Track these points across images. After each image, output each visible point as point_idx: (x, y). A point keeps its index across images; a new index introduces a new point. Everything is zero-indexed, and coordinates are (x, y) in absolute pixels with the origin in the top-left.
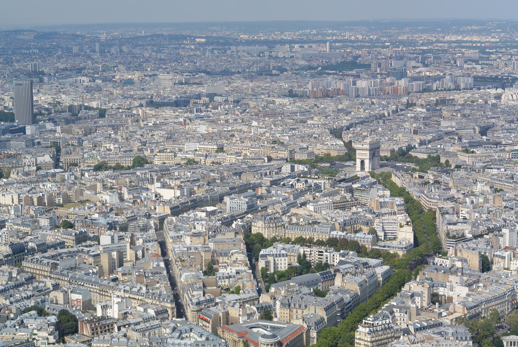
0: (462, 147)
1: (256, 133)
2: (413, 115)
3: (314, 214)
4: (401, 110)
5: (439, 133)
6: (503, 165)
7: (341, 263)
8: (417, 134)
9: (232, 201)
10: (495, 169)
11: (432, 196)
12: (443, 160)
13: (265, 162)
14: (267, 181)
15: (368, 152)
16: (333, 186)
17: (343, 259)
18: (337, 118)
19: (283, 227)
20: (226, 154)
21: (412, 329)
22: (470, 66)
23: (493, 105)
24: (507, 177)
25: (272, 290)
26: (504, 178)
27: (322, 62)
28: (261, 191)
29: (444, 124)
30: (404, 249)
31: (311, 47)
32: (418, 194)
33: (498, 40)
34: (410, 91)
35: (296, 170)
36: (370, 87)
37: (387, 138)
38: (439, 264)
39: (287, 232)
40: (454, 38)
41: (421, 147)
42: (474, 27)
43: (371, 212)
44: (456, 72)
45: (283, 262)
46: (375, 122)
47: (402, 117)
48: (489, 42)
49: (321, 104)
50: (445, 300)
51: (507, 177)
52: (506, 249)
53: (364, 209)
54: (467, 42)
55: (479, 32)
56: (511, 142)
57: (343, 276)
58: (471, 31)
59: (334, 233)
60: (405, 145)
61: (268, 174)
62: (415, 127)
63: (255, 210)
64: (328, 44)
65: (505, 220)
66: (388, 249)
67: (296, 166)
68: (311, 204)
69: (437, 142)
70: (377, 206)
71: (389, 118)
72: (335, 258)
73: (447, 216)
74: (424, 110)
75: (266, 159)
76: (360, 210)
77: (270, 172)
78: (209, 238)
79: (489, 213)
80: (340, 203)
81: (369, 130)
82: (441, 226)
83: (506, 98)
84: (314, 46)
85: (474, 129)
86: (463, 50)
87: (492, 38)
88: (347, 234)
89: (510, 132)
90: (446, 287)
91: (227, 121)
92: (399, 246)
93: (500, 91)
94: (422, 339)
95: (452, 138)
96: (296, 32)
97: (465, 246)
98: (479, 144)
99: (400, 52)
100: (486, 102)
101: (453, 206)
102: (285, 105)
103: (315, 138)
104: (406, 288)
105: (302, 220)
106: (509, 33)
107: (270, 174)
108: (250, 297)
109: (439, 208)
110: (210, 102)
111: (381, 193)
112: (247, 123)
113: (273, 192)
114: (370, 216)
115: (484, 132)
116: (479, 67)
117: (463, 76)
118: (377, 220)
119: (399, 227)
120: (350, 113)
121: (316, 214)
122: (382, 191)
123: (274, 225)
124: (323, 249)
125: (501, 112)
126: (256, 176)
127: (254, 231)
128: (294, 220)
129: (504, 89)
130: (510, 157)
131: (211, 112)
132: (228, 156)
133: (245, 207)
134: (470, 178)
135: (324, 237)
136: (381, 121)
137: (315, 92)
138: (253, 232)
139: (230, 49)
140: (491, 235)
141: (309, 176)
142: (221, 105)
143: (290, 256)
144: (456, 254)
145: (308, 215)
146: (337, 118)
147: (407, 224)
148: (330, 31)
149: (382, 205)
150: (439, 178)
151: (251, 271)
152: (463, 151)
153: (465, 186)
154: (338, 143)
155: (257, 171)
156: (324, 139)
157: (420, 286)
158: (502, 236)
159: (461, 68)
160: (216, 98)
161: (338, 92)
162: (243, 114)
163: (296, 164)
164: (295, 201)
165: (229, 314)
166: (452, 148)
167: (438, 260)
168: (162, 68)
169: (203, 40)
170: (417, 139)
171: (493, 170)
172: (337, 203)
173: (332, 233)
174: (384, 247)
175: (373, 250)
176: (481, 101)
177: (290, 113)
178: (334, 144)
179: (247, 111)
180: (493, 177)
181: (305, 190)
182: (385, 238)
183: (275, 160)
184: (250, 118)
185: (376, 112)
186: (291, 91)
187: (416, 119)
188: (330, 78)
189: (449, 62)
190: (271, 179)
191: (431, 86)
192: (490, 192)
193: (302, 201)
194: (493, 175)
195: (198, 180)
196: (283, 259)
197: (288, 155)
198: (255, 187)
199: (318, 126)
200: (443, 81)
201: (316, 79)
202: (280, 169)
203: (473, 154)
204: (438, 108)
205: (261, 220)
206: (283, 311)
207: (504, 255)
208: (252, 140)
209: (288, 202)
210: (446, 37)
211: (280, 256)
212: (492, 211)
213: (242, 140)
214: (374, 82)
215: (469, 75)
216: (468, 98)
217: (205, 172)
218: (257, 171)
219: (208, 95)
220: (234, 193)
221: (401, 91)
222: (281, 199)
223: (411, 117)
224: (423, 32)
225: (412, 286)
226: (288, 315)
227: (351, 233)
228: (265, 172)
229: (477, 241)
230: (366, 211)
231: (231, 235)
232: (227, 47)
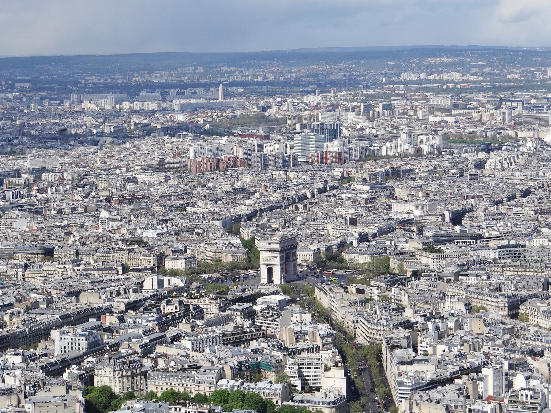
0: (424, 244)
1: (106, 228)
2: (350, 195)
3: (191, 353)
4: (332, 188)
5: (389, 221)
6: (485, 270)
8: (356, 225)
9: (63, 337)
10: (472, 275)
11: (376, 321)
12: (394, 264)
13: (118, 274)
14: (120, 304)
15: (278, 255)
16: (223, 309)
18: (233, 203)
19: (143, 377)
20: (57, 263)
22: (438, 119)
23: (473, 178)
24: (491, 287)
26: (486, 290)
27: (212, 115)
28: (110, 320)
29: (397, 207)
30: (332, 405)
31: (195, 93)
32: (355, 318)
33: (481, 78)
35: (166, 285)
36: (285, 155)
37: (308, 232)
39: (149, 383)
40: (413, 77)
41: (362, 244)
42: (445, 60)
43: (282, 348)
44: (417, 128)
46: (291, 207)
47: (333, 199)
48: (467, 81)
49: (209, 181)
51: (491, 287)
52: (489, 400)
53: (270, 344)
54: (435, 81)
56: (498, 234)
58: (440, 65)
59: (223, 382)
60: (336, 242)
61: (122, 292)
62: (352, 214)
63: (100, 350)
64: (221, 88)
65: (487, 355)
66: (307, 405)
67: (166, 279)
68: (187, 338)
69: (385, 236)
70: (290, 339)
71: (313, 200)
73: (398, 351)
74: (367, 188)
75: (120, 269)
76: (264, 345)
77: (125, 289)
78: (26, 397)
79: (463, 345)
80: (234, 334)
81: (282, 219)
82: (389, 366)
83: (493, 167)
84: (199, 90)
85: (443, 216)
86: (428, 94)
87: (472, 74)
88: (243, 384)
89: (497, 219)
91: (60, 211)
92: (324, 400)
93: (482, 155)
95: (409, 230)
97: (425, 397)
98: (449, 239)
99: (332, 99)
101: (407, 334)
102: (151, 184)
103: (198, 234)
105: (172, 363)
106: (498, 66)
107: (125, 293)
109: (386, 339)
110: (35, 181)
111: (296, 317)
112: (93, 213)
113: (129, 320)
114: (278, 355)
115: (457, 218)
116: (451, 120)
117: (427, 135)
118: (290, 361)
119: (323, 371)
120: (253, 193)
121: (195, 354)
122: (298, 315)
123: (130, 373)
125: (484, 188)
126: (104, 297)
127: (98, 382)
128: (161, 364)
129: (489, 152)
130: (497, 257)
131: (36, 197)
132: (60, 266)
133: (84, 345)
134: (434, 292)
135: (207, 389)
136: (300, 206)
137: (200, 162)
138: (96, 385)
139: (69, 99)
140: (465, 378)
141: (185, 294)
142: (51, 186)
145: (182, 356)
146: (233, 203)
147: (336, 366)
148: (225, 69)
149: (298, 336)
150: (388, 293)
152: (425, 250)
153: (427, 303)
154: (232, 242)
155: (105, 288)
156: (211, 235)
158: (482, 379)
159: (425, 121)
160: (45, 176)
161: (235, 163)
162: (86, 200)
163: (166, 275)
164: (163, 334)
166: (407, 245)
169: (27, 85)
170: (355, 232)
171: (470, 277)
172: (229, 335)
173: (220, 382)
174: (302, 401)
175: (283, 407)
176: (453, 171)
177: (161, 197)
178: (227, 242)
179: (93, 194)
180: (471, 289)
181: (180, 317)
182: (303, 388)
183: (133, 270)
184: (97, 205)
185: (294, 192)
186: (162, 163)
187: (354, 202)
188: (223, 141)
189: (407, 114)
190: (126, 301)
191: (377, 150)
192: (464, 311)
193: (175, 334)
194: (469, 286)
195: (11, 305)
197: (155, 261)
198: (99, 314)
199: (203, 216)
200: (396, 143)
201: (202, 142)
202: (141, 284)
204: (387, 184)
205: (109, 365)
208: (98, 239)
209: (153, 336)
210: (402, 75)
212: (466, 342)
213: (83, 240)
214: (291, 145)
215: (436, 132)
216: (434, 167)
217: (22, 292)
218: (105, 288)
219: (32, 171)
220: (68, 324)
221: (331, 158)
222: (141, 332)
223: (349, 199)
227: (251, 382)
228: (117, 289)
229: (444, 388)
230: (273, 346)
231: (60, 390)
232: (64, 95)
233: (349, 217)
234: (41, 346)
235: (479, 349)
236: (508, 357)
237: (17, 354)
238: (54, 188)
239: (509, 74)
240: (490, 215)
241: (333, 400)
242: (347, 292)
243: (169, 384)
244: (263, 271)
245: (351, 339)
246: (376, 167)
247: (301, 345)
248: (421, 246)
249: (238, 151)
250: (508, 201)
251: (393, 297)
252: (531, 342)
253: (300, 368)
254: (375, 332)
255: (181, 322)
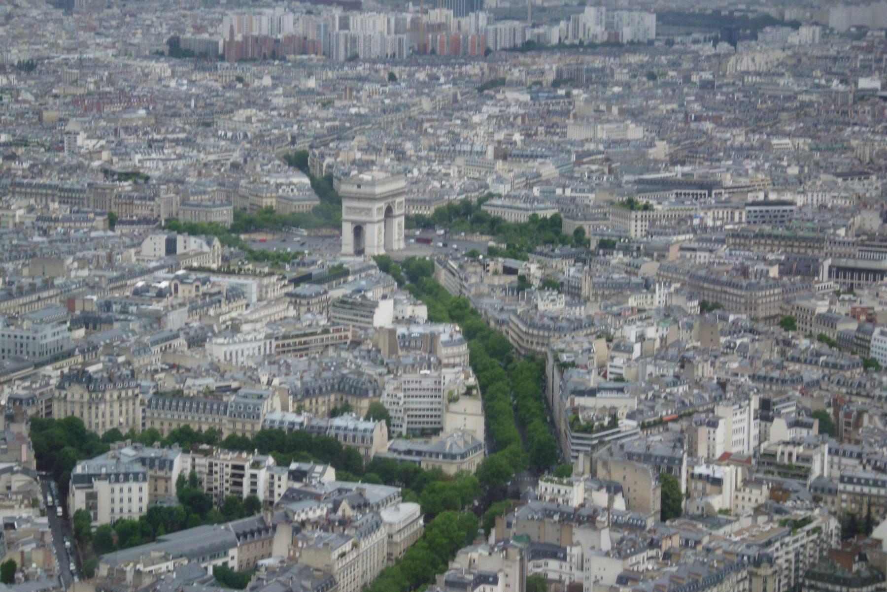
7: (292, 496)
17: (297, 485)
25: (103, 570)
34: (491, 45)
35: (180, 249)
38: (548, 498)
39: (148, 414)
45: (135, 495)
66: (417, 458)
67: (180, 239)
72: (276, 483)
76: (344, 354)
90: (564, 559)
93: (724, 47)
100: (687, 79)
104: (460, 563)
124: (247, 459)
125: (724, 103)
129: (733, 43)
135: (248, 427)
143: (156, 479)
144: (593, 473)
163: (179, 233)
167: (546, 487)
171: (698, 254)
172: (285, 337)
176: (672, 73)
196: (135, 486)
200: (576, 21)
203: (648, 213)
207: (718, 475)
211: (126, 478)
243: (183, 418)
244: (347, 230)
251: (566, 283)
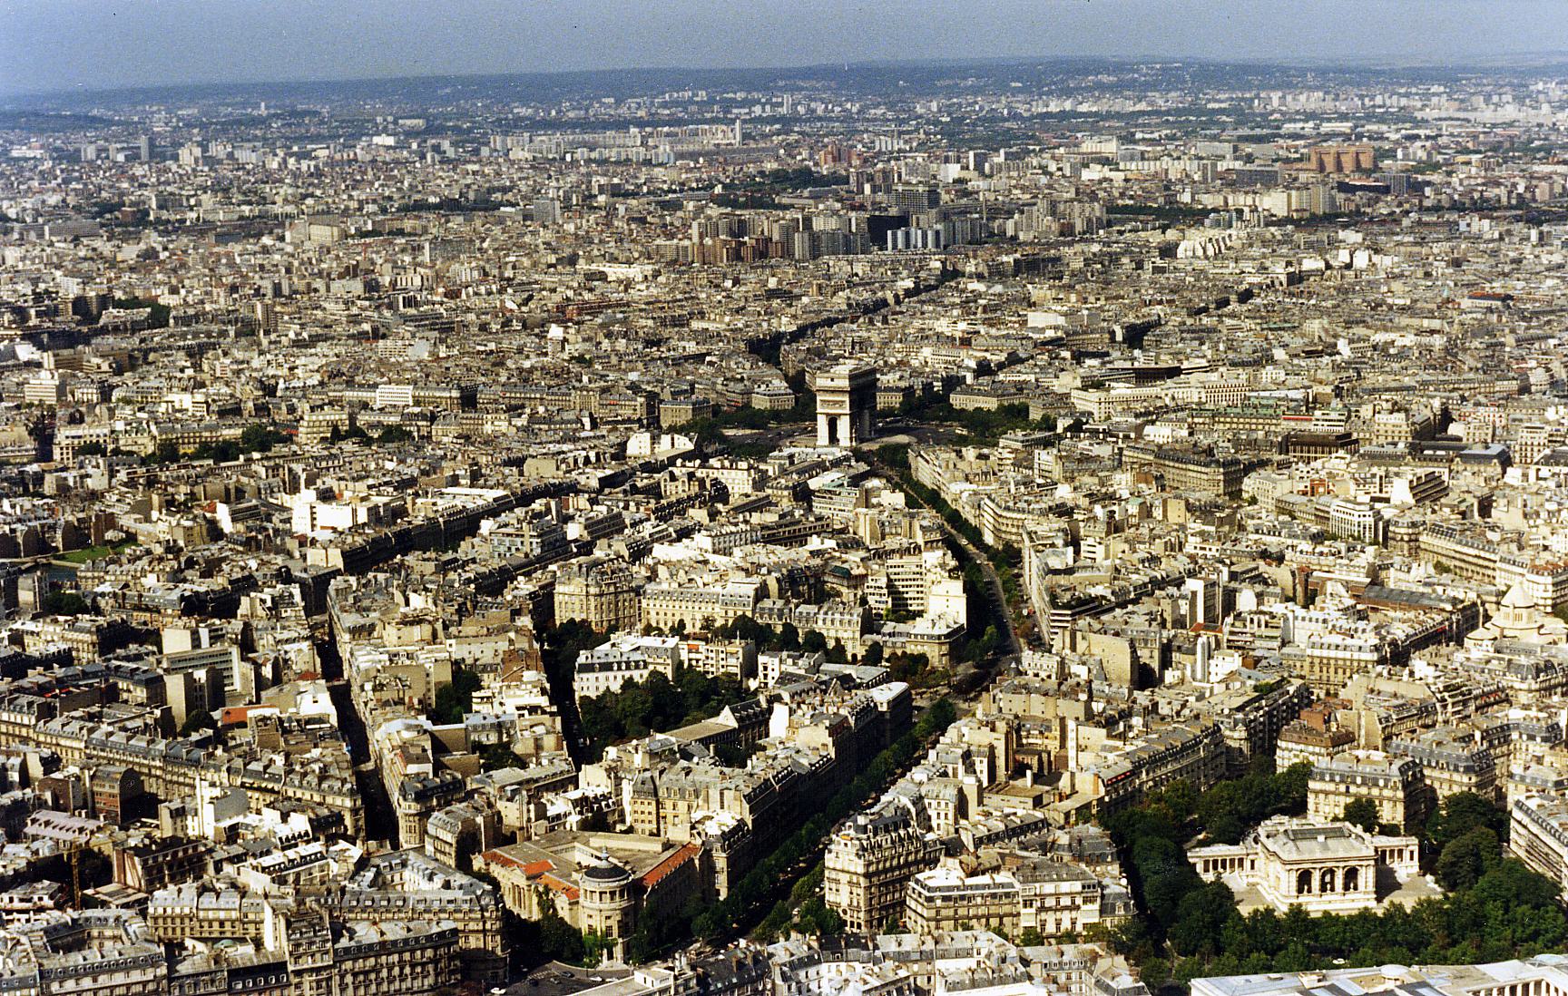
3: (712, 558)
4: (929, 288)
15: (846, 398)
21: (967, 838)
22: (1096, 176)
29: (1036, 319)
30: (943, 640)
40: (1054, 107)
42: (1105, 78)
46: (861, 320)
50: (1050, 762)
55: (1117, 89)
56: (1204, 363)
57: (792, 712)
61: (593, 459)
62: (963, 332)
65: (1193, 558)
68: (703, 532)
71: (898, 309)
77: (598, 455)
80: (781, 526)
85: (1113, 333)
94: (995, 864)
96: (656, 97)
97: (1097, 626)
102: (628, 284)
103: (711, 364)
108: (554, 775)
112: (537, 331)
120: (799, 297)
151: (554, 709)
157: (986, 730)
162: (524, 309)
165: (500, 819)
168: (312, 195)
169: (420, 123)
199: (718, 334)
206: (638, 807)
224: (976, 91)
225: (965, 730)
226: (654, 818)
228: (584, 453)
233: (958, 335)
234: (464, 546)
235: (1180, 550)
236: (1228, 561)
237: (429, 560)
238: (470, 289)
239: (1209, 101)
240: (1188, 331)
241: (946, 631)
242: (961, 457)
245: (975, 535)
246: (999, 254)
247: (891, 543)
248: (1078, 383)
249: (770, 230)
250: (1217, 308)
252: (1264, 537)
253: (890, 580)
254: (1010, 522)
255: (693, 506)
